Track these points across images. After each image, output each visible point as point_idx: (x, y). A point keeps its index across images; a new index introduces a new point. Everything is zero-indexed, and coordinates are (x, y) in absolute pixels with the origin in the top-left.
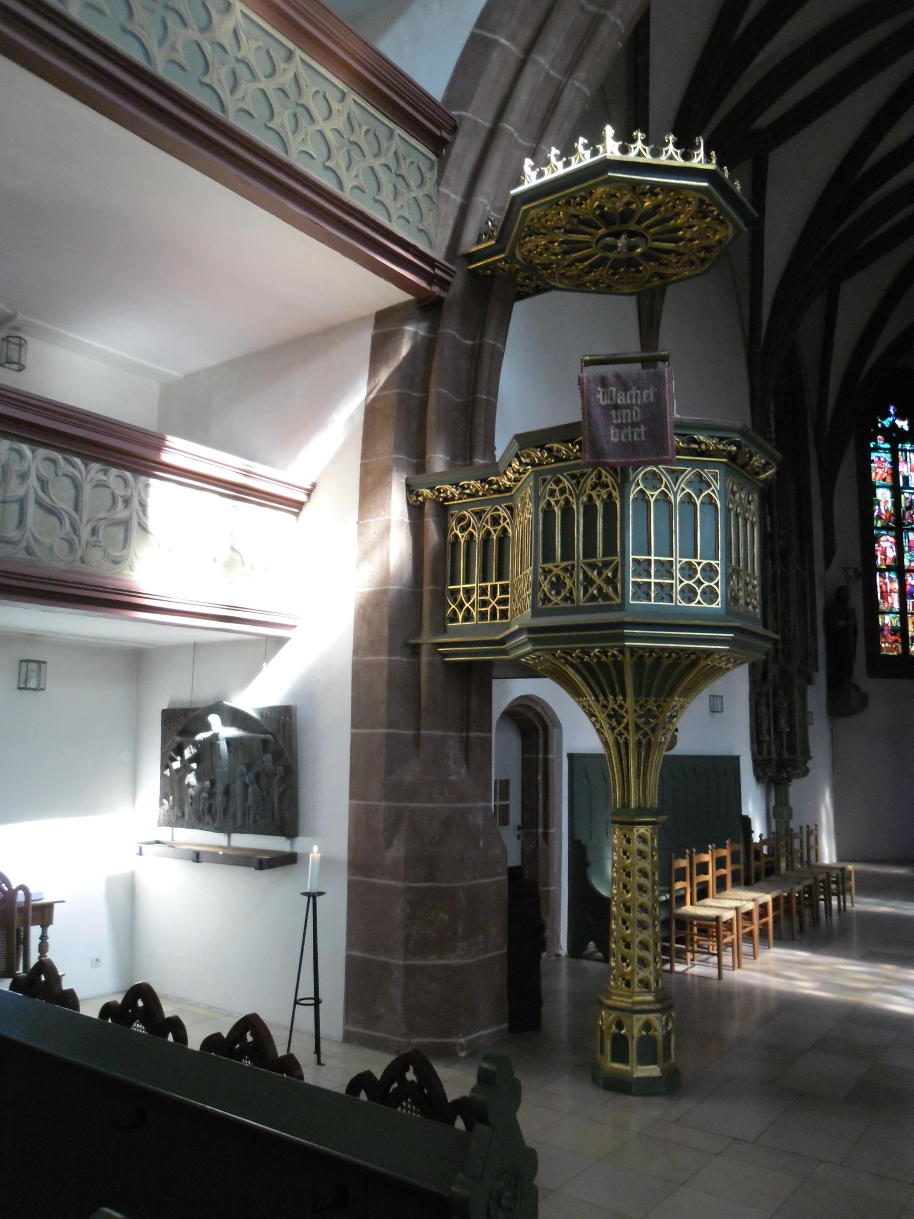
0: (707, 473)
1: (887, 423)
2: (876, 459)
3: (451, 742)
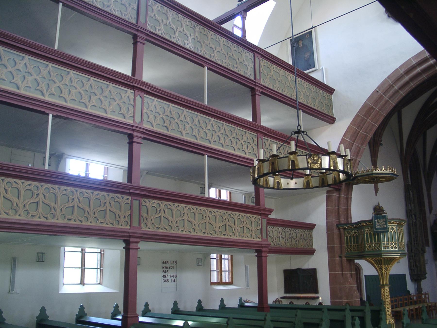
0: (394, 227)
3: (348, 274)
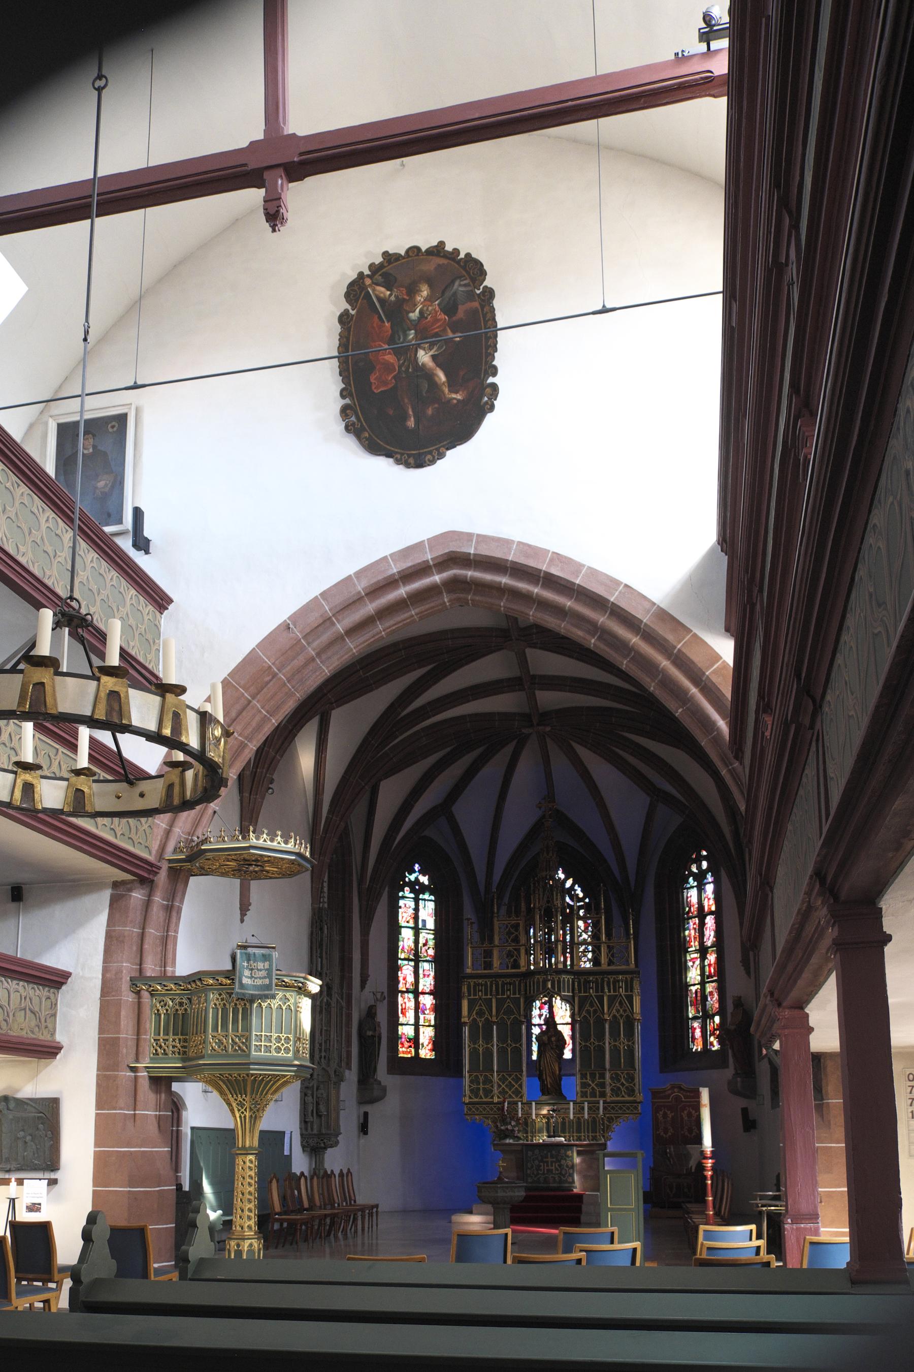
1: (412, 877)
2: (403, 906)
